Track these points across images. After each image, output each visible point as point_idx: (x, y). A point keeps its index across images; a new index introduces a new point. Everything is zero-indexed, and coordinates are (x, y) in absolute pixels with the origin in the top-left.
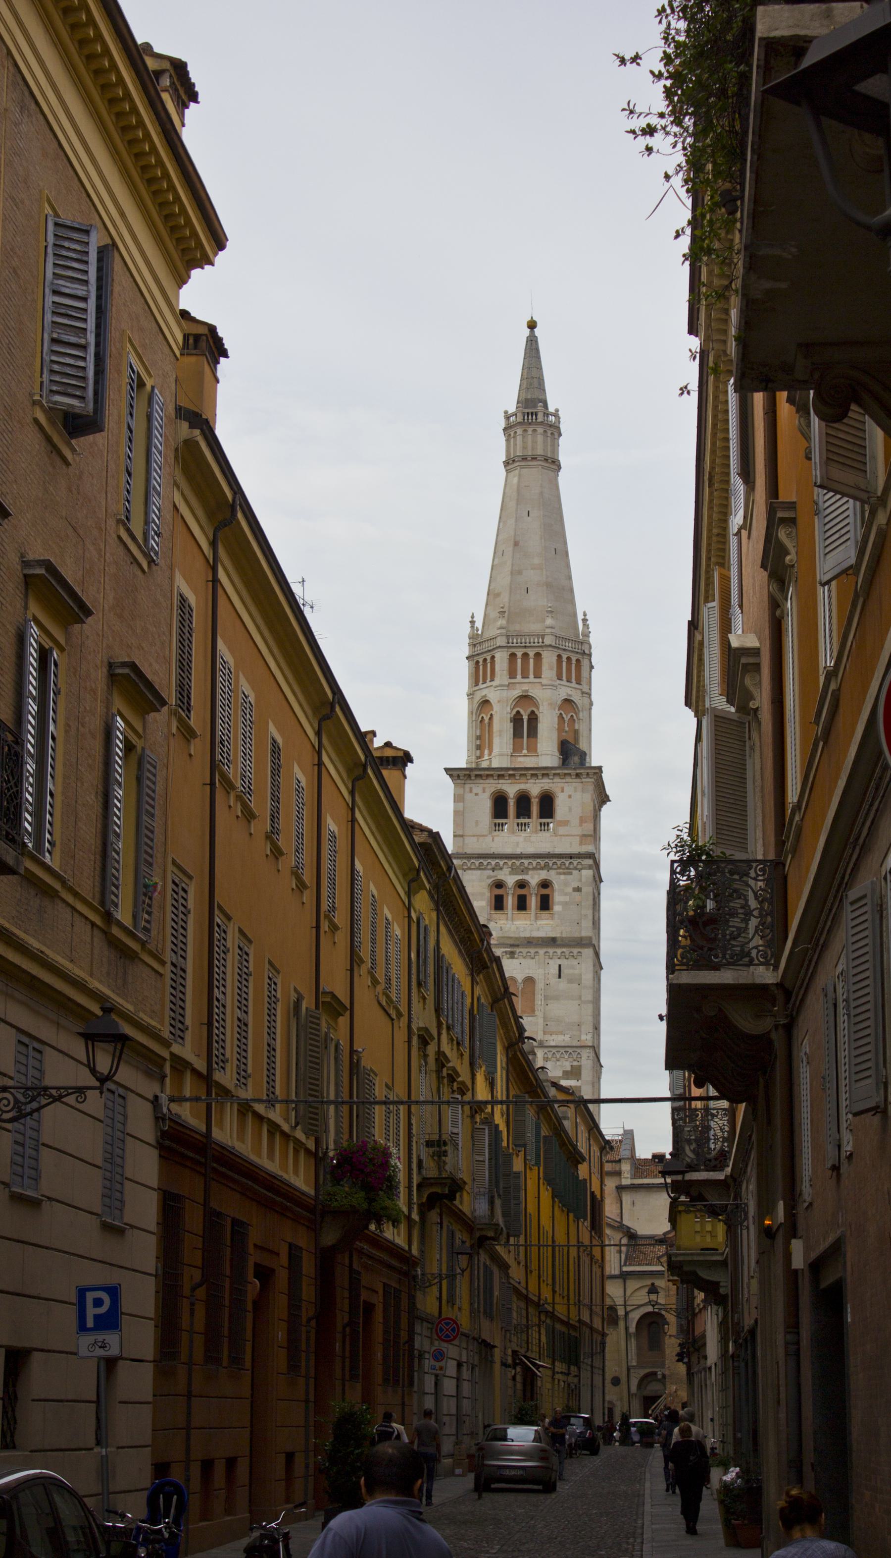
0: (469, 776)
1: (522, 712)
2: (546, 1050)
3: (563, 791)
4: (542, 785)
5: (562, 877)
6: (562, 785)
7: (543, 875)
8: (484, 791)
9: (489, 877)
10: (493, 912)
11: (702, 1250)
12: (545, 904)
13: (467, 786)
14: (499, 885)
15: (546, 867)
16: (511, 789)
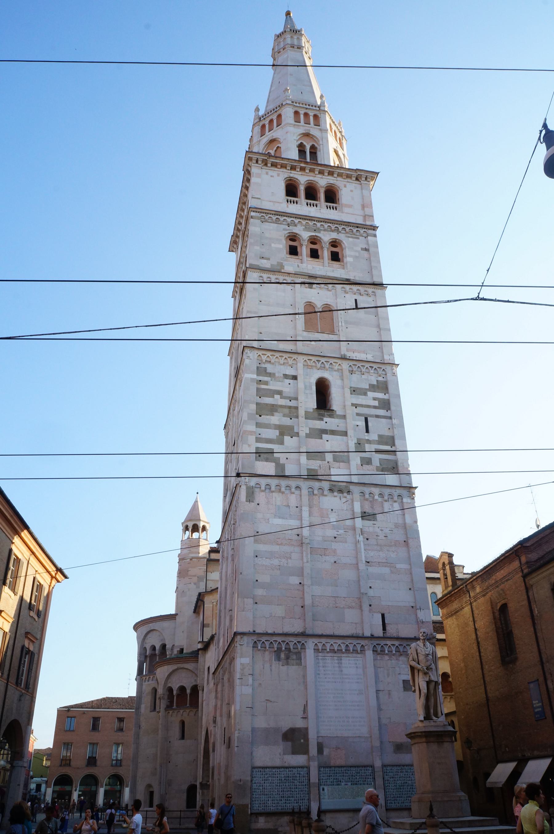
0: (266, 165)
1: (305, 143)
2: (351, 363)
3: (345, 186)
4: (328, 180)
5: (351, 239)
6: (345, 183)
7: (334, 235)
8: (278, 175)
9: (284, 230)
10: (288, 256)
11: (230, 738)
12: (335, 257)
13: (264, 171)
14: (293, 238)
15: (337, 230)
16: (302, 179)
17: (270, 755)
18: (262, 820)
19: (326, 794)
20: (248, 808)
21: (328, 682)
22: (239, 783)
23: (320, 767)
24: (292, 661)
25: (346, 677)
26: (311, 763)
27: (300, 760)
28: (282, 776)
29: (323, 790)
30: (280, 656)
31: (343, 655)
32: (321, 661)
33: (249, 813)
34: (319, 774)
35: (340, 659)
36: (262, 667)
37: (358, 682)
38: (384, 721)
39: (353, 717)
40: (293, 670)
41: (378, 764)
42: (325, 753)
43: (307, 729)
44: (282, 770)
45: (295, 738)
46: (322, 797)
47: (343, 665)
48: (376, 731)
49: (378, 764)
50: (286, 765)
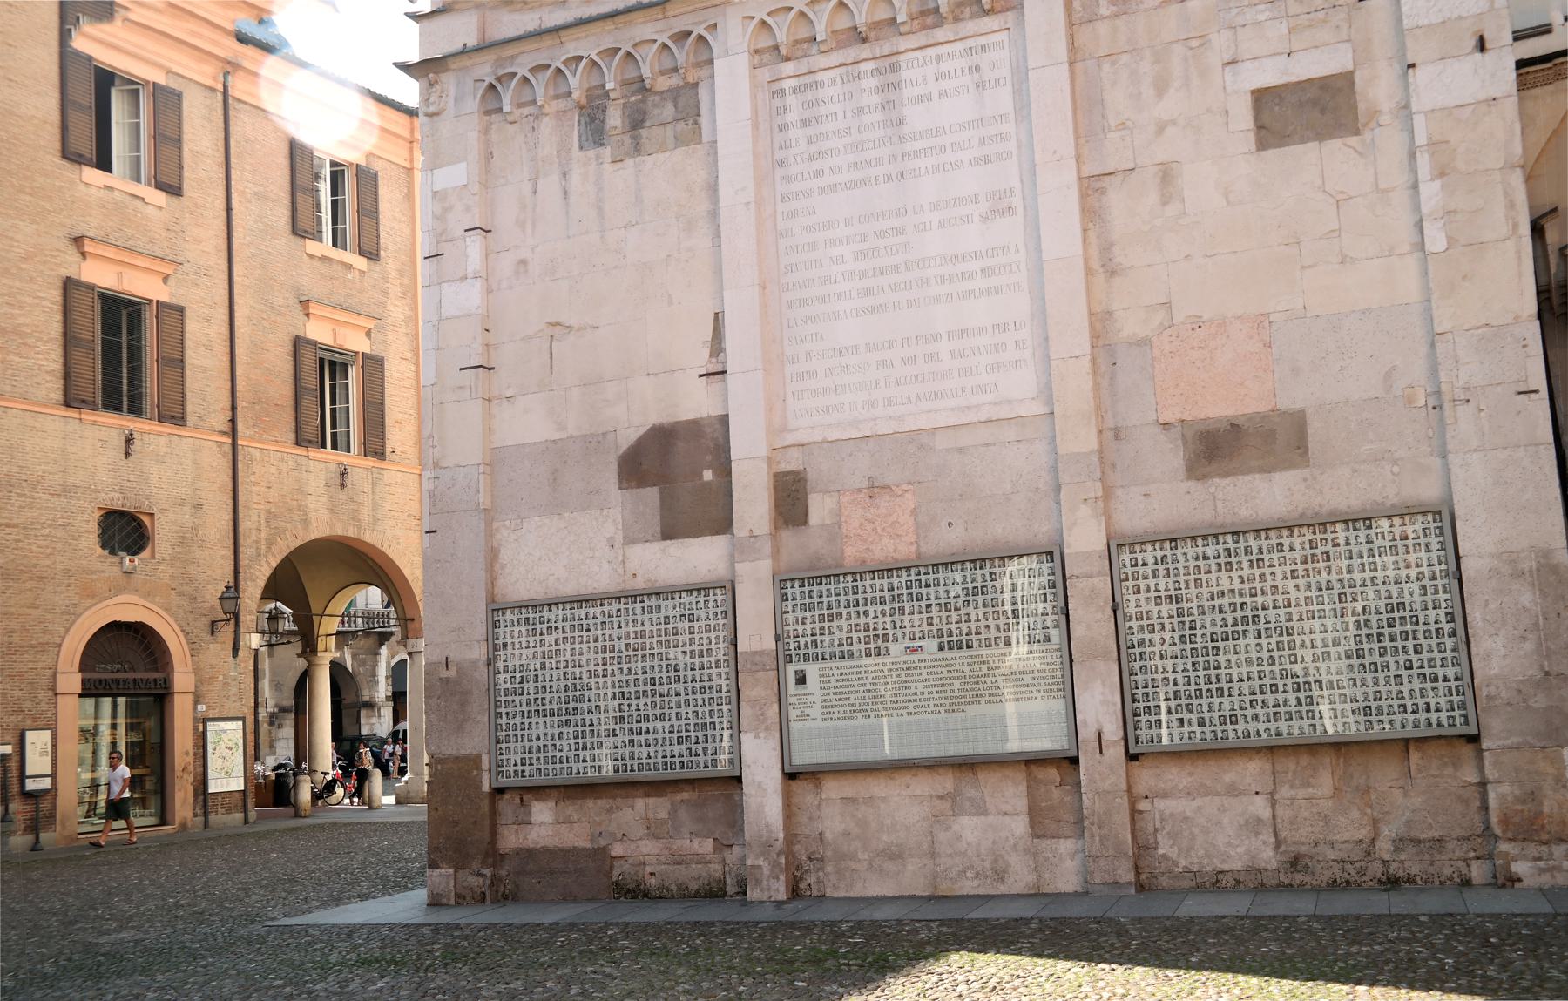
17: (584, 546)
18: (542, 812)
19: (817, 698)
20: (479, 768)
21: (831, 189)
22: (444, 674)
23: (781, 583)
24: (657, 130)
25: (919, 145)
26: (742, 568)
27: (700, 557)
28: (616, 633)
29: (801, 680)
30: (603, 122)
31: (903, 43)
32: (791, 100)
33: (486, 788)
34: (779, 615)
35: (890, 65)
36: (527, 188)
37: (987, 160)
38: (1130, 325)
39: (962, 333)
40: (664, 171)
41: (1085, 539)
42: (814, 518)
43: (724, 420)
44: (615, 606)
45: (674, 471)
46: (793, 714)
47: (908, 92)
48: (1076, 386)
49: (1085, 539)
50: (639, 584)
